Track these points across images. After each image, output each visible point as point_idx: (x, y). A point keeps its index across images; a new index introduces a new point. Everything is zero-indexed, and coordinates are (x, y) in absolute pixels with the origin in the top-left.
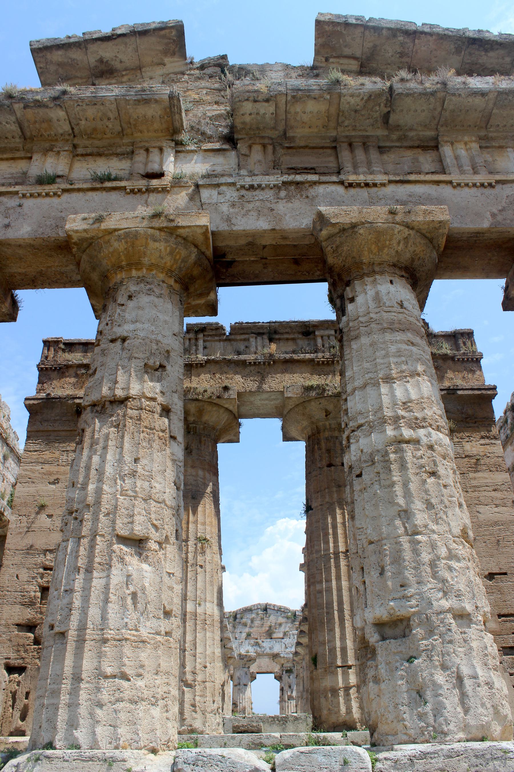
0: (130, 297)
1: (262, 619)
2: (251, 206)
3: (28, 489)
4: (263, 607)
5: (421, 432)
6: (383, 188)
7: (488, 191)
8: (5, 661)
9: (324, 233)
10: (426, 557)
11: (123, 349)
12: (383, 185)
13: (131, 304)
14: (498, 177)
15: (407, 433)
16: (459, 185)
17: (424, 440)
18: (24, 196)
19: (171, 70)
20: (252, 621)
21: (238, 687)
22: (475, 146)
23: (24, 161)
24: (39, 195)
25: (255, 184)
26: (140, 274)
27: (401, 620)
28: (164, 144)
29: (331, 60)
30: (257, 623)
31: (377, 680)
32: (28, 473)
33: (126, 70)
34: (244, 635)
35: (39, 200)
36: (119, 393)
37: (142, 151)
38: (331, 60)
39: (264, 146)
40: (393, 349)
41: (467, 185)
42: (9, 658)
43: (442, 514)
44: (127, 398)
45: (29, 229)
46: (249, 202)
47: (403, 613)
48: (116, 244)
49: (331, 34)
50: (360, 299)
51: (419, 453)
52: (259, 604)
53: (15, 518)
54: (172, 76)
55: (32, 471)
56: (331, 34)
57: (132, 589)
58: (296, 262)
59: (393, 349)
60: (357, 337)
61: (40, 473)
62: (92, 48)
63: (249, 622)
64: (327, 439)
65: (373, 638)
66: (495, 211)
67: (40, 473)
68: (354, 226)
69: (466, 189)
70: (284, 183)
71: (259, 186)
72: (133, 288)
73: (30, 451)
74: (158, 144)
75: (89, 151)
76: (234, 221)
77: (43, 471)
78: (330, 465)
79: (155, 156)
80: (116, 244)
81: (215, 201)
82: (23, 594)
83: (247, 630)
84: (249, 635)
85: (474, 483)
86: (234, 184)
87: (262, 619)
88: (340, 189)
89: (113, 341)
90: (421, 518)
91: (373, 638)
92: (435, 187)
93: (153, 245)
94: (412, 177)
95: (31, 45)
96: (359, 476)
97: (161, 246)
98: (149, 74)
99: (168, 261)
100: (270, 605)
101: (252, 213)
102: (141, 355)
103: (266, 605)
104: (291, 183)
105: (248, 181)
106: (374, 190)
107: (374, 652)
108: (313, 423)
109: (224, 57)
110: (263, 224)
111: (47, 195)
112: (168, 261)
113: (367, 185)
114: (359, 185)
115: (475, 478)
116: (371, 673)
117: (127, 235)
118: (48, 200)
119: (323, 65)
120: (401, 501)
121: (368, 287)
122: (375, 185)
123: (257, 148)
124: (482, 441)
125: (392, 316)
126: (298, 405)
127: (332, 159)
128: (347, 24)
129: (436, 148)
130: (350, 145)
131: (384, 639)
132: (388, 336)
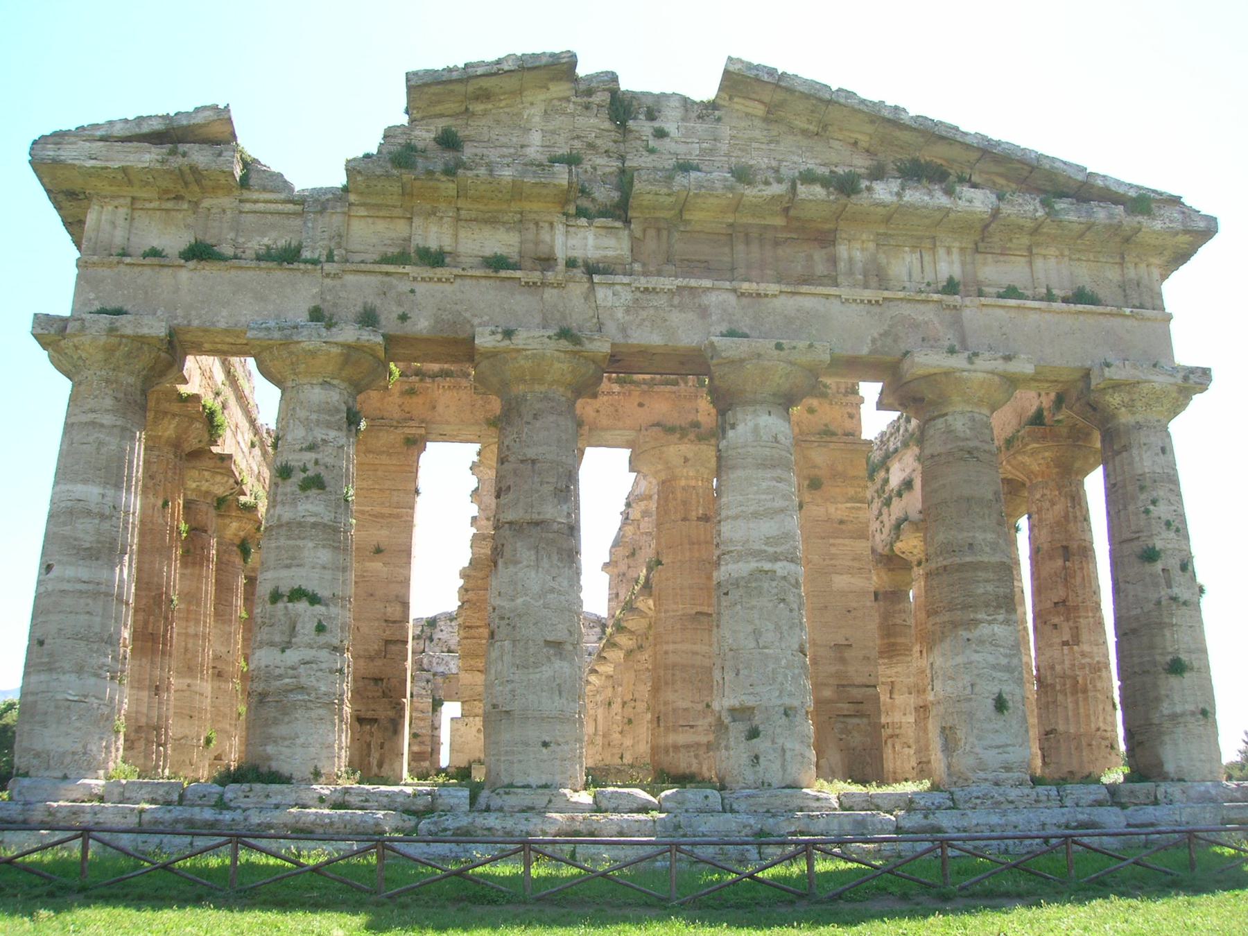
0: (535, 417)
2: (644, 314)
5: (779, 564)
6: (775, 300)
7: (876, 309)
9: (714, 361)
10: (771, 666)
11: (533, 471)
12: (775, 296)
13: (538, 424)
14: (887, 294)
15: (767, 566)
16: (847, 300)
17: (780, 573)
18: (415, 279)
19: (555, 95)
22: (871, 246)
23: (402, 221)
24: (431, 279)
25: (650, 286)
26: (543, 388)
27: (749, 708)
28: (556, 219)
29: (736, 100)
31: (727, 748)
33: (504, 93)
35: (431, 285)
36: (536, 517)
37: (532, 226)
38: (736, 100)
39: (659, 230)
40: (764, 485)
41: (855, 301)
43: (785, 634)
44: (542, 522)
45: (426, 324)
46: (643, 308)
47: (751, 704)
48: (522, 362)
49: (739, 80)
50: (741, 428)
51: (774, 584)
54: (556, 103)
56: (739, 80)
57: (558, 681)
58: (682, 363)
59: (764, 485)
60: (734, 468)
62: (474, 81)
64: (683, 488)
65: (727, 720)
66: (876, 335)
68: (742, 361)
69: (854, 305)
70: (680, 288)
71: (654, 289)
72: (538, 406)
74: (549, 218)
75: (473, 215)
76: (629, 331)
78: (684, 519)
79: (545, 236)
80: (522, 362)
81: (610, 304)
85: (833, 550)
86: (629, 285)
88: (732, 298)
89: (522, 461)
90: (769, 637)
91: (727, 720)
92: (823, 300)
93: (557, 365)
94: (804, 289)
95: (408, 80)
96: (727, 594)
97: (565, 366)
98: (530, 99)
99: (569, 377)
101: (646, 323)
102: (551, 480)
104: (684, 288)
105: (643, 282)
106: (766, 300)
107: (727, 728)
108: (669, 468)
109: (613, 78)
110: (654, 339)
111: (440, 280)
112: (569, 377)
113: (759, 295)
114: (750, 295)
115: (834, 545)
116: (724, 743)
117: (534, 355)
118: (440, 284)
119: (726, 103)
120: (757, 622)
121: (749, 417)
122: (766, 295)
123: (652, 233)
124: (849, 505)
125: (767, 451)
127: (727, 250)
128: (757, 80)
129: (833, 243)
130: (747, 235)
131: (734, 721)
132: (760, 473)
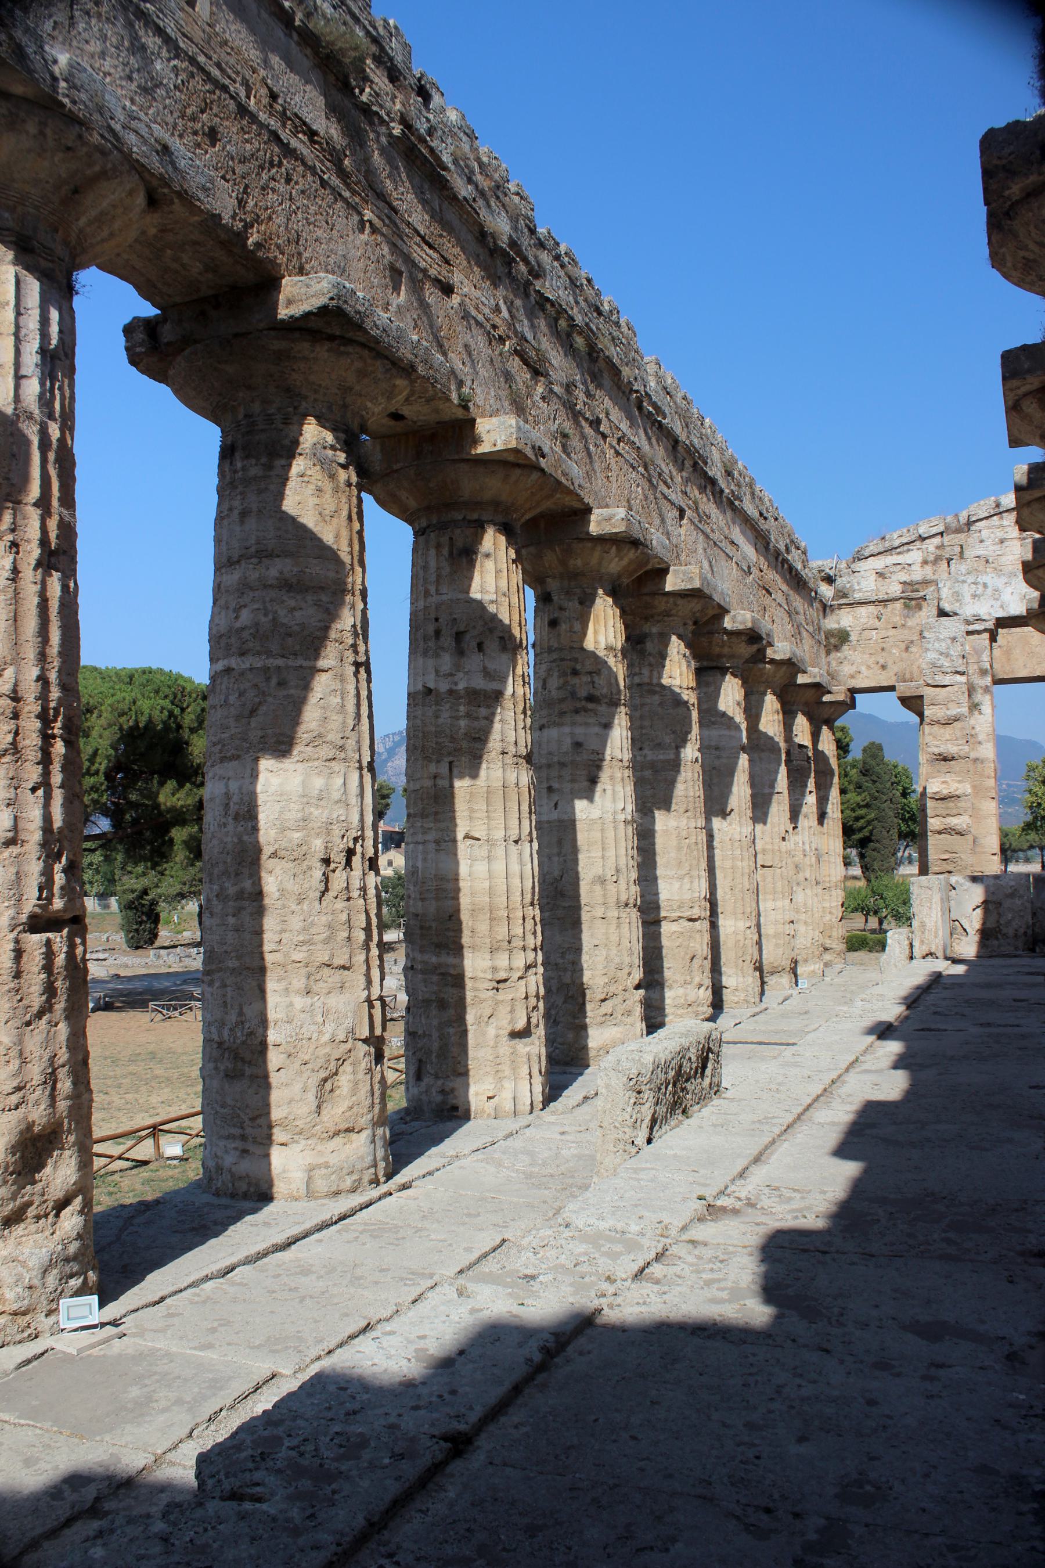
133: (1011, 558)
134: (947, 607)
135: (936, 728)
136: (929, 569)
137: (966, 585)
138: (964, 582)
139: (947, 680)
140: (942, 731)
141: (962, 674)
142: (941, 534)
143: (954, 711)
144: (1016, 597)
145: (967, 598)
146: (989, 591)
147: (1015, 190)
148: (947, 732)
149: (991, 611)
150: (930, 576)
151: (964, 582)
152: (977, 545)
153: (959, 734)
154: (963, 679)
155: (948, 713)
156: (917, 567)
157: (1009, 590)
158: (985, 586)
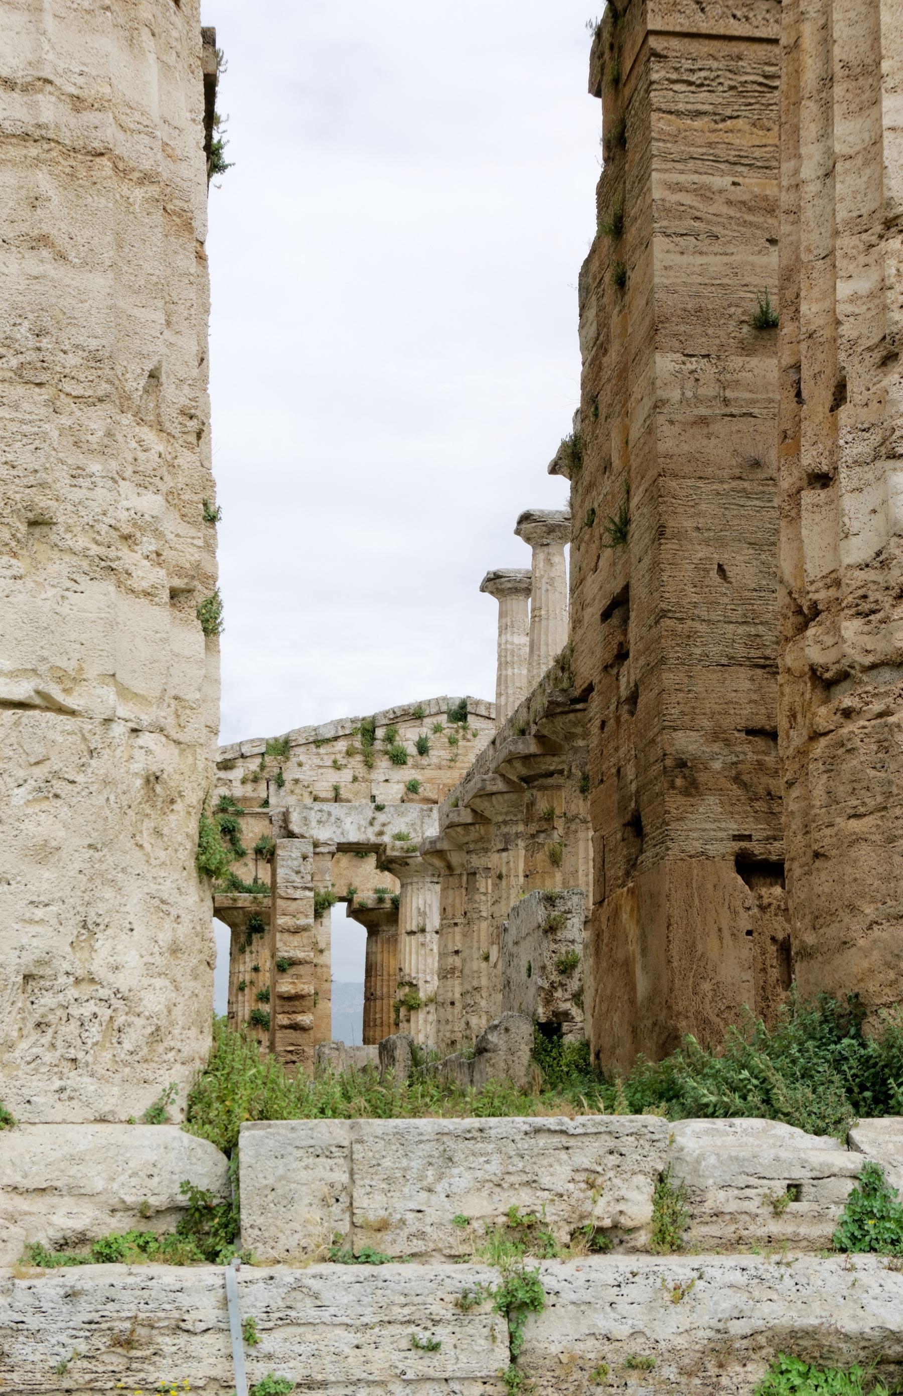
1: (453, 742)
3: (700, 260)
4: (454, 707)
8: (737, 846)
20: (422, 749)
21: (420, 937)
30: (438, 753)
32: (687, 199)
34: (396, 790)
42: (749, 838)
52: (445, 699)
53: (671, 366)
55: (704, 193)
61: (729, 203)
63: (412, 750)
67: (729, 203)
73: (678, 113)
77: (738, 194)
82: (753, 631)
83: (407, 774)
84: (413, 788)
87: (453, 742)
100: (477, 703)
103: (463, 705)
126: (877, 39)
133: (325, 784)
134: (295, 828)
135: (286, 935)
136: (249, 787)
137: (313, 812)
138: (311, 809)
139: (298, 894)
140: (291, 938)
141: (310, 889)
142: (263, 754)
143: (302, 921)
144: (355, 827)
145: (314, 824)
146: (333, 819)
147: (559, 710)
148: (295, 940)
149: (333, 836)
150: (250, 794)
151: (311, 809)
152: (297, 769)
153: (305, 941)
154: (311, 894)
155: (298, 922)
156: (236, 783)
157: (349, 820)
158: (329, 814)
